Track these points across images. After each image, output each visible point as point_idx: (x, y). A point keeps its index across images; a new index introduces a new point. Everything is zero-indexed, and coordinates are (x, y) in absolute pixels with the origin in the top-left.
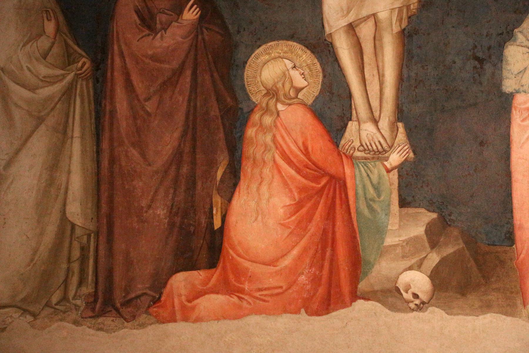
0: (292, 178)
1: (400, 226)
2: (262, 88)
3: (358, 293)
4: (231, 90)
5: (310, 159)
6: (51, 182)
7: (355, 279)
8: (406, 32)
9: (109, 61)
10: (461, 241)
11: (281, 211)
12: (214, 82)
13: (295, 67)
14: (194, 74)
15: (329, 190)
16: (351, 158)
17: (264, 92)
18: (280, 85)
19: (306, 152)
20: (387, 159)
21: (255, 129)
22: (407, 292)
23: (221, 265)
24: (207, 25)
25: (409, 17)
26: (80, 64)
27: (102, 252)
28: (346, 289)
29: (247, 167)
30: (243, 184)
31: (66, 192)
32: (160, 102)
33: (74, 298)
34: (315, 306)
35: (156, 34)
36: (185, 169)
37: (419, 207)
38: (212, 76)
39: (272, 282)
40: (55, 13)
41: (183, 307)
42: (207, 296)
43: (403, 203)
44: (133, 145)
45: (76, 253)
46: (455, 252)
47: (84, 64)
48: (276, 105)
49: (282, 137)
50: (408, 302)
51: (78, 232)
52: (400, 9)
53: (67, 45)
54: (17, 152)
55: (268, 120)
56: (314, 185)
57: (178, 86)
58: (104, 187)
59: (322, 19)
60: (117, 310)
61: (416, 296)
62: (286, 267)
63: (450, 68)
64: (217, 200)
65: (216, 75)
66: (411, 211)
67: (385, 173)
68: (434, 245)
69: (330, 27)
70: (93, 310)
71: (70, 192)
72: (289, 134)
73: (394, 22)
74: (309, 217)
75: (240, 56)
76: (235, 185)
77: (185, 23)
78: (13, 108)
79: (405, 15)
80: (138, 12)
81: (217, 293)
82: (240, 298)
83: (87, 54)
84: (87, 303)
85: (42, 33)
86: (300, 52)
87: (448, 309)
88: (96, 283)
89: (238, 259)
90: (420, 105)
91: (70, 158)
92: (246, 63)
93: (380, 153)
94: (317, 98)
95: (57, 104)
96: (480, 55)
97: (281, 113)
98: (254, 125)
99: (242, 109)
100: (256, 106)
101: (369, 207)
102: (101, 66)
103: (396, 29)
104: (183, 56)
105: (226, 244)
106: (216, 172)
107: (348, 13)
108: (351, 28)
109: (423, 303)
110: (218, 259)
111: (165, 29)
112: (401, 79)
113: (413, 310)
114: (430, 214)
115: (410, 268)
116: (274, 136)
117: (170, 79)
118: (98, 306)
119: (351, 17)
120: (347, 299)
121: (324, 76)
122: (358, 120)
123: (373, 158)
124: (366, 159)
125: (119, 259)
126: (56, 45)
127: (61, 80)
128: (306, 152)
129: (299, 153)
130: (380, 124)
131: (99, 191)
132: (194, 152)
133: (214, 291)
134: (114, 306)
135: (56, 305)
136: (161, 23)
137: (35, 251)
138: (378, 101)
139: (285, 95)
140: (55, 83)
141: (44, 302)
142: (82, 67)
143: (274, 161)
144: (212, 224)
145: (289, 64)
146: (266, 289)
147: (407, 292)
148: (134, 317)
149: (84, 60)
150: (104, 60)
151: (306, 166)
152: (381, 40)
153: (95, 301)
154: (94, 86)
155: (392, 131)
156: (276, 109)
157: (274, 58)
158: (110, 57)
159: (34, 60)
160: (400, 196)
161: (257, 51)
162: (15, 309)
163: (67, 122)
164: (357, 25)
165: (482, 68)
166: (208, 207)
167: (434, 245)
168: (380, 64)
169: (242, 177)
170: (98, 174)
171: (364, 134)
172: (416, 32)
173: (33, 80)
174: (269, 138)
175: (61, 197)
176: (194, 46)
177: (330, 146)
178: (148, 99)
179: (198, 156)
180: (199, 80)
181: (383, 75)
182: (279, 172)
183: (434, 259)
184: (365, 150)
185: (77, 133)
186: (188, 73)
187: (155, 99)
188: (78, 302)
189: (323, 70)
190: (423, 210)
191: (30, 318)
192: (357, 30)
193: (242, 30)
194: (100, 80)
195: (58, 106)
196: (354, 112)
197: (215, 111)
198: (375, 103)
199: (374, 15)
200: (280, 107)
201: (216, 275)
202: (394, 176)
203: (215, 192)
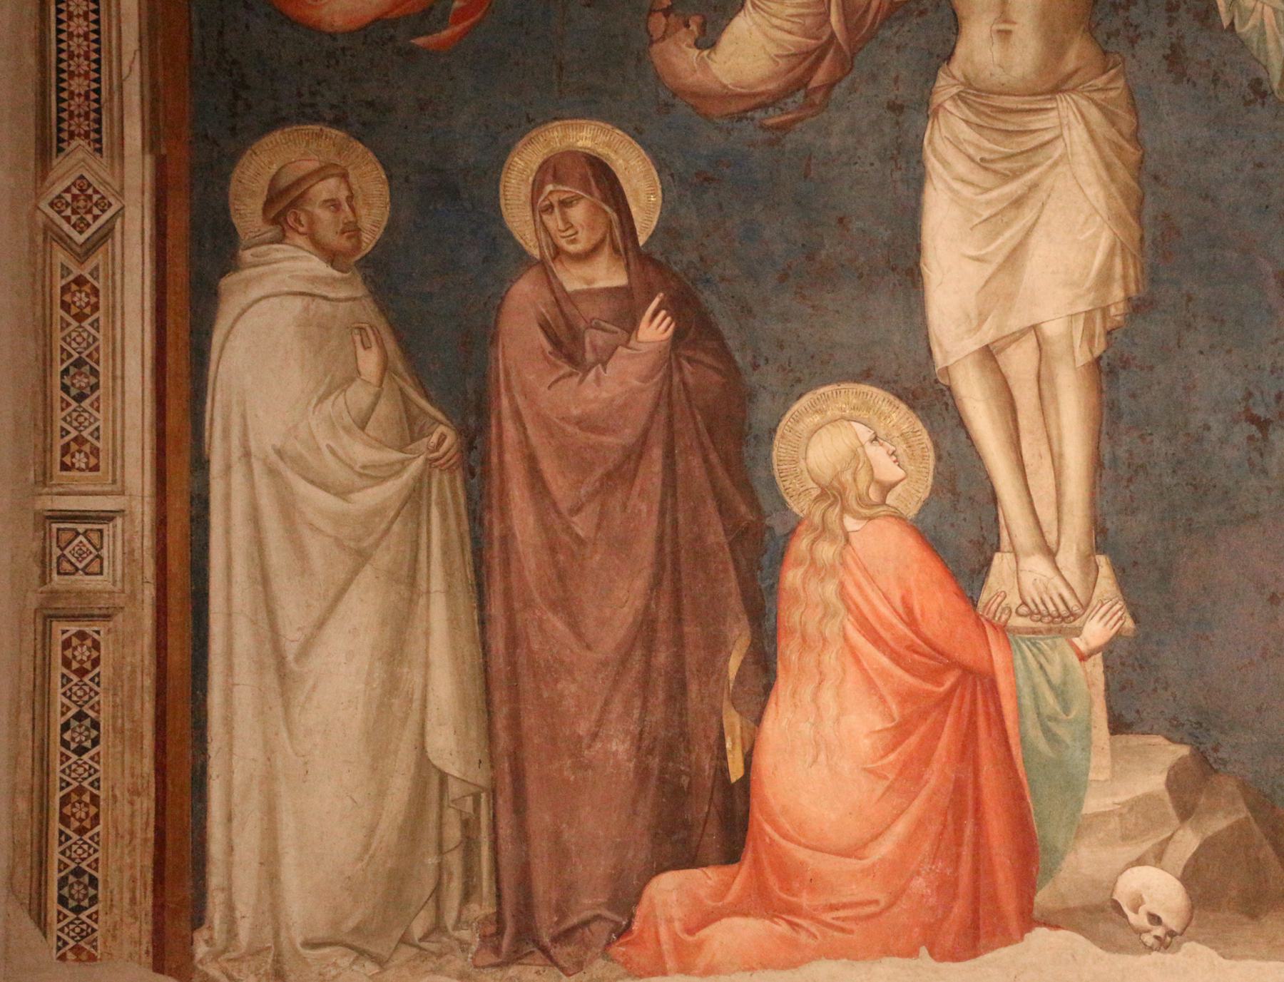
0: (883, 673)
1: (1113, 773)
2: (812, 484)
3: (1036, 914)
4: (746, 487)
5: (917, 633)
6: (392, 684)
7: (1027, 882)
8: (1103, 363)
9: (494, 430)
10: (1241, 804)
11: (865, 744)
12: (710, 469)
13: (876, 439)
14: (669, 455)
15: (962, 697)
16: (1003, 629)
17: (816, 492)
18: (847, 477)
19: (911, 620)
20: (1078, 632)
21: (801, 571)
22: (1136, 911)
23: (748, 856)
24: (690, 353)
25: (1109, 333)
26: (434, 438)
27: (505, 831)
28: (1010, 906)
29: (789, 652)
30: (783, 687)
31: (424, 706)
32: (603, 515)
33: (456, 928)
34: (948, 942)
35: (587, 372)
36: (662, 657)
37: (1150, 732)
38: (706, 460)
39: (856, 891)
40: (377, 333)
41: (678, 945)
42: (725, 922)
43: (1118, 725)
44: (553, 606)
45: (454, 834)
46: (1231, 828)
47: (442, 438)
48: (841, 519)
49: (859, 586)
50: (1139, 932)
51: (454, 789)
52: (1089, 315)
53: (405, 398)
54: (321, 624)
55: (826, 551)
56: (929, 687)
57: (638, 482)
58: (499, 696)
59: (927, 337)
60: (544, 950)
61: (1155, 919)
62: (882, 860)
63: (1199, 440)
64: (733, 721)
65: (714, 457)
66: (1134, 740)
67: (1076, 660)
68: (1185, 812)
69: (946, 354)
70: (497, 950)
71: (431, 707)
72: (872, 580)
73: (1077, 341)
74: (924, 756)
75: (760, 414)
76: (768, 689)
77: (644, 348)
78: (306, 533)
79: (1099, 329)
80: (545, 327)
81: (746, 914)
82: (790, 923)
83: (444, 413)
84: (483, 937)
85: (354, 374)
86: (885, 408)
87: (1224, 945)
88: (499, 896)
89: (783, 842)
90: (1143, 517)
91: (427, 634)
92: (773, 431)
93: (1063, 619)
94: (926, 503)
95: (392, 522)
96: (1260, 411)
97: (853, 537)
98: (799, 563)
99: (770, 528)
100: (800, 522)
101: (1047, 732)
102: (478, 441)
103: (1083, 357)
104: (643, 419)
105: (756, 814)
106: (727, 661)
107: (980, 325)
108: (989, 355)
109: (1171, 934)
110: (743, 843)
111: (604, 360)
112: (1097, 465)
113: (1151, 949)
114: (1173, 747)
115: (1140, 862)
116: (842, 585)
117: (618, 468)
118: (506, 942)
119: (988, 334)
120: (1013, 924)
121: (939, 458)
122: (1014, 551)
123: (1050, 630)
124: (1034, 631)
125: (541, 846)
126: (382, 401)
127: (398, 473)
128: (911, 620)
129: (895, 620)
130: (1060, 558)
131: (489, 703)
132: (677, 618)
133: (738, 910)
134: (537, 942)
135: (421, 940)
136: (594, 348)
137: (372, 830)
138: (1053, 510)
139: (859, 498)
140: (384, 479)
141: (398, 934)
142: (440, 443)
143: (846, 638)
144: (723, 771)
145: (865, 434)
146: (844, 906)
147: (1136, 911)
148: (580, 966)
149: (442, 429)
150: (482, 429)
151: (912, 648)
152: (1052, 381)
153: (500, 932)
154: (465, 481)
155: (1086, 574)
156: (843, 527)
157: (833, 421)
158: (493, 422)
159: (342, 432)
160: (1110, 709)
161: (797, 407)
162: (341, 950)
163: (415, 560)
164: (1003, 349)
165: (1265, 438)
166: (714, 736)
167: (1185, 812)
168: (1054, 433)
169: (781, 674)
170: (486, 669)
171: (1027, 580)
172: (1126, 364)
173: (341, 475)
174: (831, 589)
175: (415, 717)
176: (665, 398)
177: (961, 606)
178: (577, 510)
179: (686, 629)
180: (680, 467)
181: (1061, 456)
182: (857, 661)
183: (1188, 842)
184: (1031, 614)
185: (437, 583)
186: (657, 453)
187: (592, 510)
188: (465, 934)
189: (936, 445)
190: (1159, 740)
191: (371, 968)
192: (1001, 359)
193: (762, 362)
194: (478, 470)
195: (396, 527)
196: (1004, 534)
197: (716, 535)
198: (1047, 515)
199: (1035, 328)
200: (851, 523)
201: (741, 874)
202: (1096, 667)
203: (726, 704)
